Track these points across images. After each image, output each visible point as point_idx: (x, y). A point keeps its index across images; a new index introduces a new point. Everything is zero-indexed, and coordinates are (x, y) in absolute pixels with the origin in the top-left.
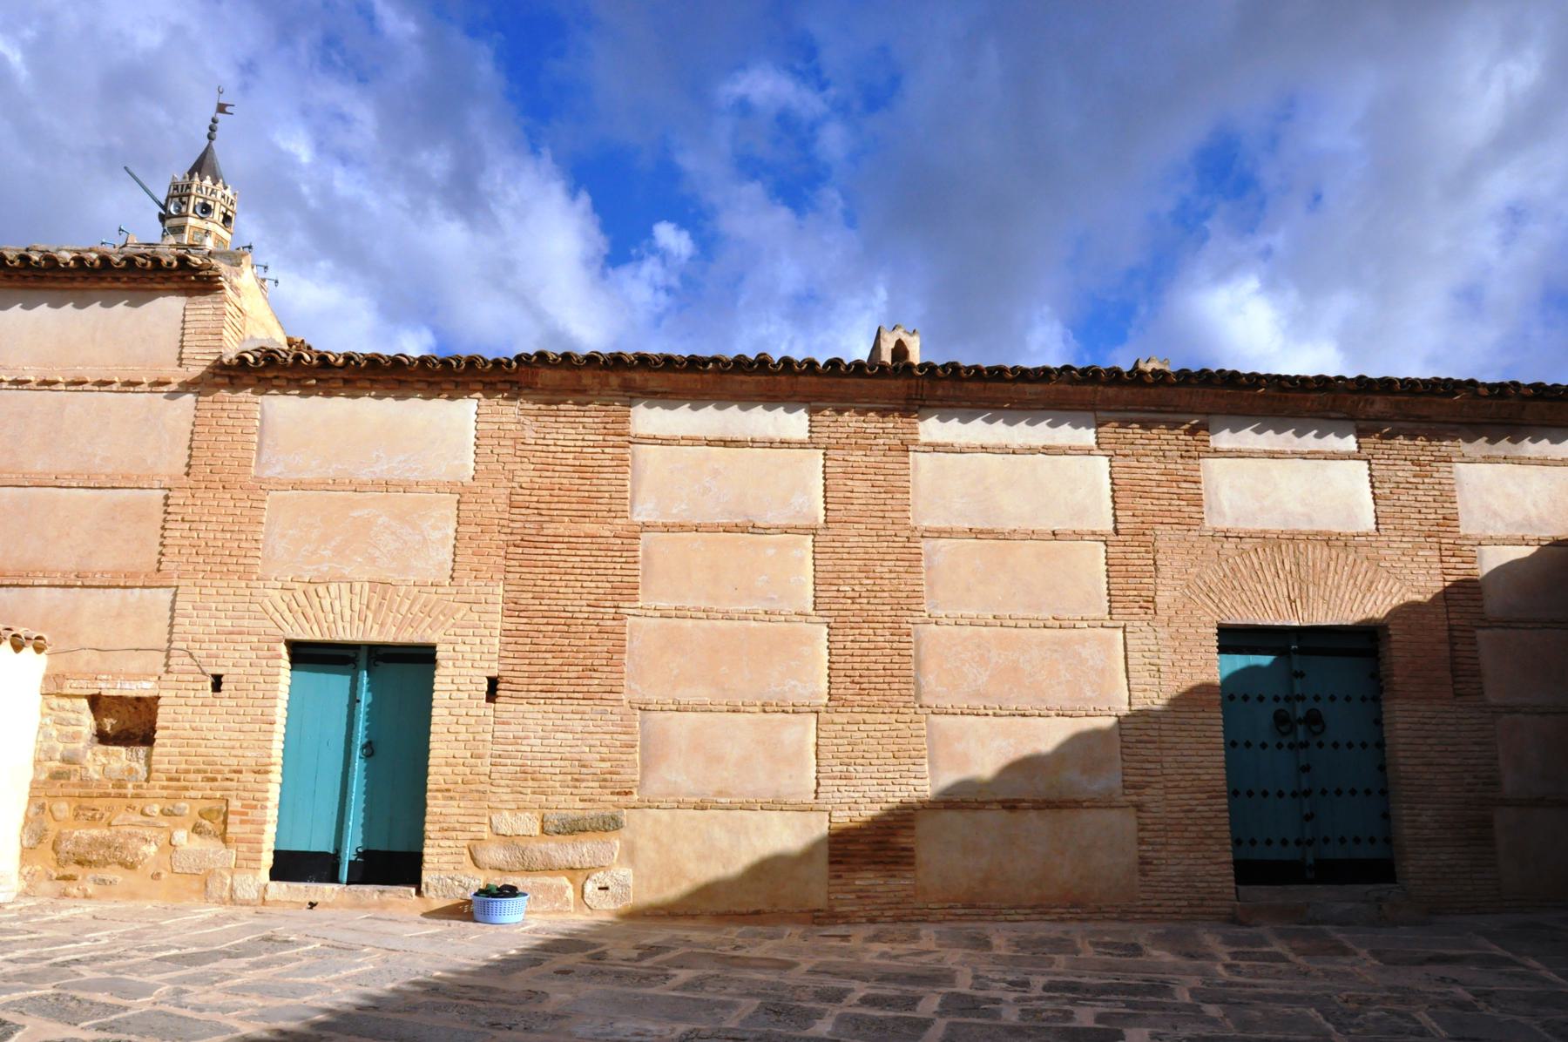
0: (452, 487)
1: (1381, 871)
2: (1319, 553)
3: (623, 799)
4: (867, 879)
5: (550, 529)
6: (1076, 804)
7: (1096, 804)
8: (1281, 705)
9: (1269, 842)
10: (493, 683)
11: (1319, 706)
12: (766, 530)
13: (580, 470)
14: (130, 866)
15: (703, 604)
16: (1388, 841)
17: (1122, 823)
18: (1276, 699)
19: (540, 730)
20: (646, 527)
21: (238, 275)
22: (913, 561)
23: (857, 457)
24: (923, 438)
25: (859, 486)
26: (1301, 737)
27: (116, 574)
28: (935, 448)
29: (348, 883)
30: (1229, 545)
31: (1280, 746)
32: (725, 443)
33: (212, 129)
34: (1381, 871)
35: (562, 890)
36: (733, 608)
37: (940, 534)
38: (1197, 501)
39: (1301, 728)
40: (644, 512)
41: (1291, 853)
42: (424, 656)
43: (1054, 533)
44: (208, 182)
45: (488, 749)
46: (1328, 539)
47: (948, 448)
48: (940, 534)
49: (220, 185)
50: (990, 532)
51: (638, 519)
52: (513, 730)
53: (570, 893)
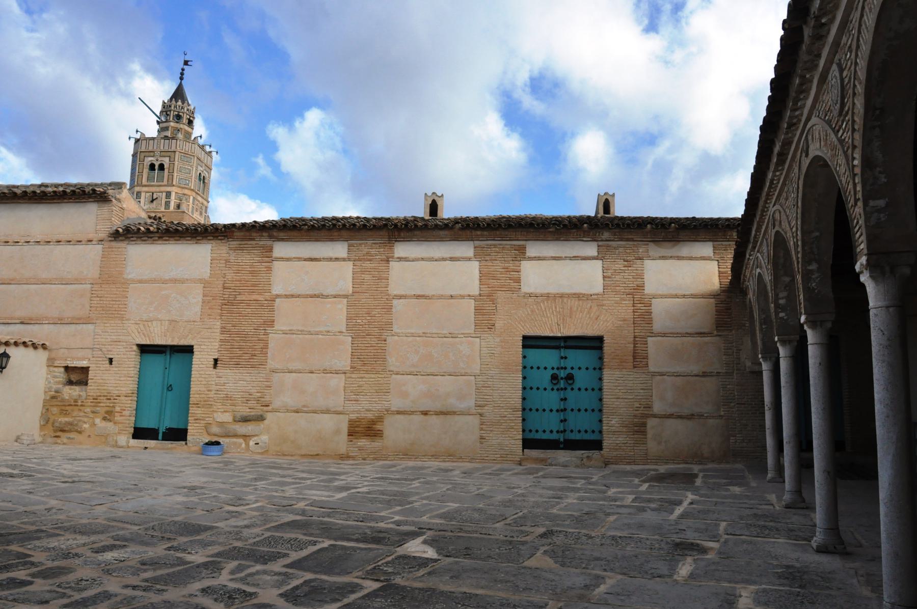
0: (201, 281)
1: (597, 445)
2: (575, 303)
3: (265, 408)
4: (363, 442)
5: (239, 298)
6: (454, 413)
7: (462, 414)
8: (555, 371)
9: (544, 431)
10: (216, 360)
11: (573, 372)
12: (327, 296)
13: (252, 272)
14: (80, 432)
15: (300, 328)
16: (601, 432)
17: (473, 421)
18: (553, 368)
19: (234, 381)
20: (278, 296)
21: (120, 193)
22: (389, 309)
23: (367, 264)
24: (396, 255)
25: (367, 277)
26: (562, 386)
27: (73, 318)
28: (400, 259)
29: (163, 440)
30: (530, 300)
31: (553, 389)
32: (311, 260)
33: (182, 74)
34: (597, 445)
35: (241, 444)
36: (312, 330)
37: (401, 297)
38: (518, 281)
39: (562, 382)
40: (277, 289)
41: (554, 436)
42: (188, 350)
44: (180, 103)
45: (214, 388)
46: (578, 296)
47: (406, 259)
48: (401, 297)
49: (186, 104)
51: (274, 293)
52: (222, 380)
53: (243, 445)
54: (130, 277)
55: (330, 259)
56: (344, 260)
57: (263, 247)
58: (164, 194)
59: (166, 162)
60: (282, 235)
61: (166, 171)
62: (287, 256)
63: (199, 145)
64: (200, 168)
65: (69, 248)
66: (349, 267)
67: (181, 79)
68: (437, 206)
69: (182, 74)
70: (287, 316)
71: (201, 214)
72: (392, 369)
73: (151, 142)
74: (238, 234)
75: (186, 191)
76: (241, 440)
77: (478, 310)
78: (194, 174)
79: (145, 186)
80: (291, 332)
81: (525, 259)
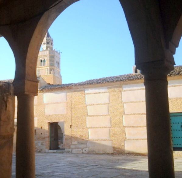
10: (71, 126)
37: (126, 103)
44: (48, 38)
58: (46, 70)
59: (46, 58)
60: (87, 86)
61: (46, 62)
63: (56, 51)
71: (58, 74)
74: (74, 87)
76: (80, 149)
78: (55, 62)
79: (40, 67)
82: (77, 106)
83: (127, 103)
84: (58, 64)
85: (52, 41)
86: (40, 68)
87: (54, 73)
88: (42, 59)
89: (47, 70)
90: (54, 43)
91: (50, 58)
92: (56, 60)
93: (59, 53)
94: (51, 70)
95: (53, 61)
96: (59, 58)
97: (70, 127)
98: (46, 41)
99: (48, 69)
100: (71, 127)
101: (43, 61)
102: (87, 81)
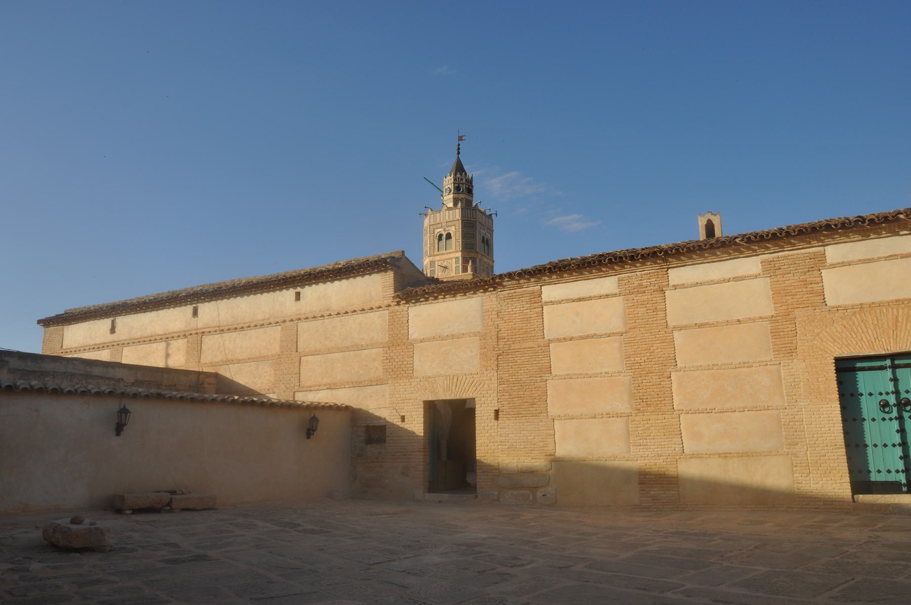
5: (513, 347)
10: (497, 412)
12: (601, 336)
20: (550, 341)
28: (675, 287)
32: (580, 300)
33: (459, 149)
37: (680, 328)
40: (548, 335)
43: (739, 321)
44: (458, 176)
47: (683, 286)
48: (680, 328)
50: (707, 324)
54: (414, 337)
55: (600, 297)
56: (615, 295)
57: (533, 293)
61: (453, 238)
62: (558, 298)
63: (480, 211)
64: (482, 231)
65: (360, 317)
66: (618, 302)
67: (459, 153)
68: (713, 226)
69: (459, 149)
70: (561, 359)
71: (488, 273)
72: (681, 407)
73: (438, 215)
75: (473, 255)
76: (527, 492)
77: (775, 333)
80: (569, 377)
81: (825, 267)
82: (516, 346)
83: (686, 327)
84: (488, 244)
85: (471, 183)
86: (437, 258)
87: (475, 270)
88: (443, 233)
89: (457, 262)
90: (474, 191)
91: (462, 228)
92: (480, 232)
93: (491, 215)
94: (465, 261)
95: (473, 236)
96: (491, 231)
97: (493, 414)
98: (454, 183)
99: (458, 258)
100: (497, 417)
101: (444, 236)
102: (550, 263)
